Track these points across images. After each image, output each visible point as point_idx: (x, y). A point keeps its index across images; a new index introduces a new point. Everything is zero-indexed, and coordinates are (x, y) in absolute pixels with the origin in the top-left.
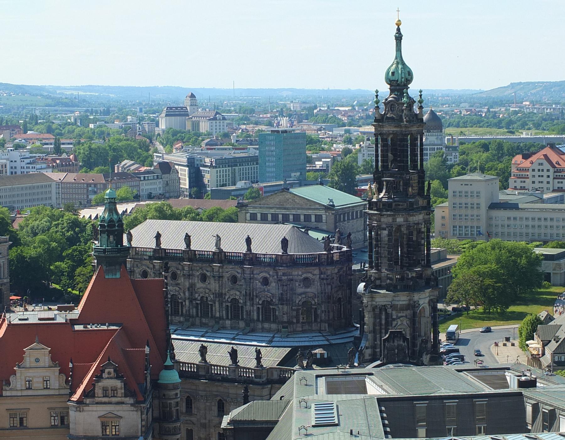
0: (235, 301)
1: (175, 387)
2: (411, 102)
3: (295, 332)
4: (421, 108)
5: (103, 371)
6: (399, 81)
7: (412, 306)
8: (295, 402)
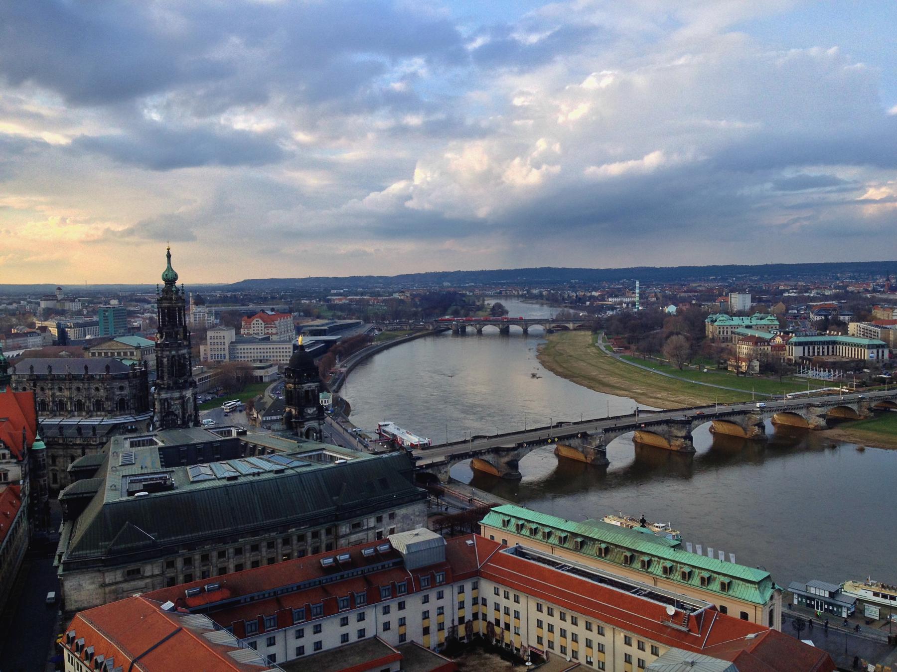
0: (79, 401)
1: (42, 450)
3: (116, 416)
6: (170, 279)
7: (182, 398)
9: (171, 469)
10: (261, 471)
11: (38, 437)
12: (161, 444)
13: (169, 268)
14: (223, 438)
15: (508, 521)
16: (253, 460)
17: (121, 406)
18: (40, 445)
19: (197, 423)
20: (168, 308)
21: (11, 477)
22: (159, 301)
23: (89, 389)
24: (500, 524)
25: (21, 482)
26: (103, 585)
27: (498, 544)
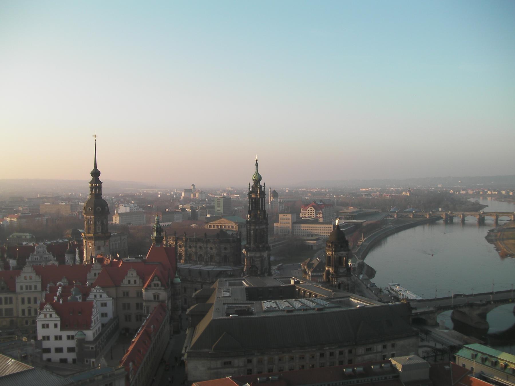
0: (201, 255)
1: (179, 284)
2: (261, 187)
4: (264, 189)
5: (154, 278)
6: (258, 180)
7: (261, 257)
8: (217, 289)
9: (252, 302)
10: (308, 308)
11: (177, 275)
12: (247, 286)
13: (257, 172)
14: (285, 285)
15: (476, 355)
16: (304, 300)
17: (225, 260)
18: (178, 280)
19: (270, 274)
20: (255, 198)
21: (161, 298)
22: (250, 193)
23: (207, 247)
24: (470, 357)
25: (166, 302)
26: (209, 369)
27: (467, 370)
